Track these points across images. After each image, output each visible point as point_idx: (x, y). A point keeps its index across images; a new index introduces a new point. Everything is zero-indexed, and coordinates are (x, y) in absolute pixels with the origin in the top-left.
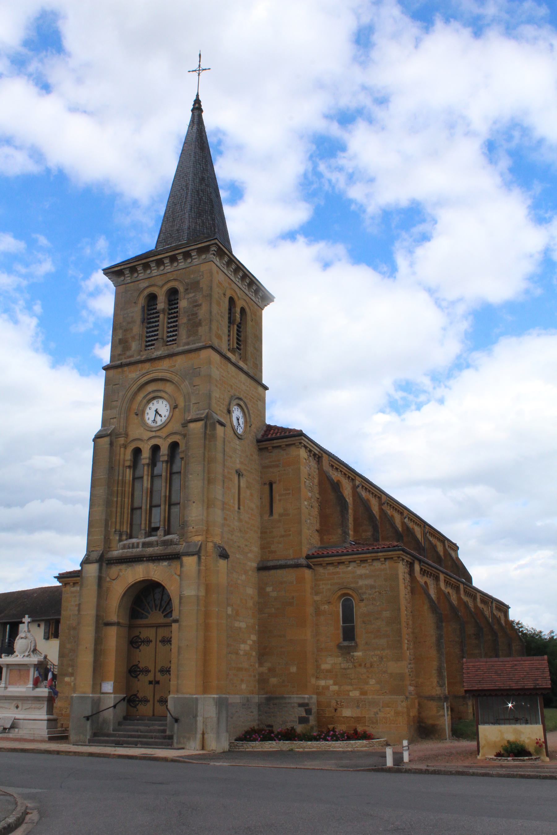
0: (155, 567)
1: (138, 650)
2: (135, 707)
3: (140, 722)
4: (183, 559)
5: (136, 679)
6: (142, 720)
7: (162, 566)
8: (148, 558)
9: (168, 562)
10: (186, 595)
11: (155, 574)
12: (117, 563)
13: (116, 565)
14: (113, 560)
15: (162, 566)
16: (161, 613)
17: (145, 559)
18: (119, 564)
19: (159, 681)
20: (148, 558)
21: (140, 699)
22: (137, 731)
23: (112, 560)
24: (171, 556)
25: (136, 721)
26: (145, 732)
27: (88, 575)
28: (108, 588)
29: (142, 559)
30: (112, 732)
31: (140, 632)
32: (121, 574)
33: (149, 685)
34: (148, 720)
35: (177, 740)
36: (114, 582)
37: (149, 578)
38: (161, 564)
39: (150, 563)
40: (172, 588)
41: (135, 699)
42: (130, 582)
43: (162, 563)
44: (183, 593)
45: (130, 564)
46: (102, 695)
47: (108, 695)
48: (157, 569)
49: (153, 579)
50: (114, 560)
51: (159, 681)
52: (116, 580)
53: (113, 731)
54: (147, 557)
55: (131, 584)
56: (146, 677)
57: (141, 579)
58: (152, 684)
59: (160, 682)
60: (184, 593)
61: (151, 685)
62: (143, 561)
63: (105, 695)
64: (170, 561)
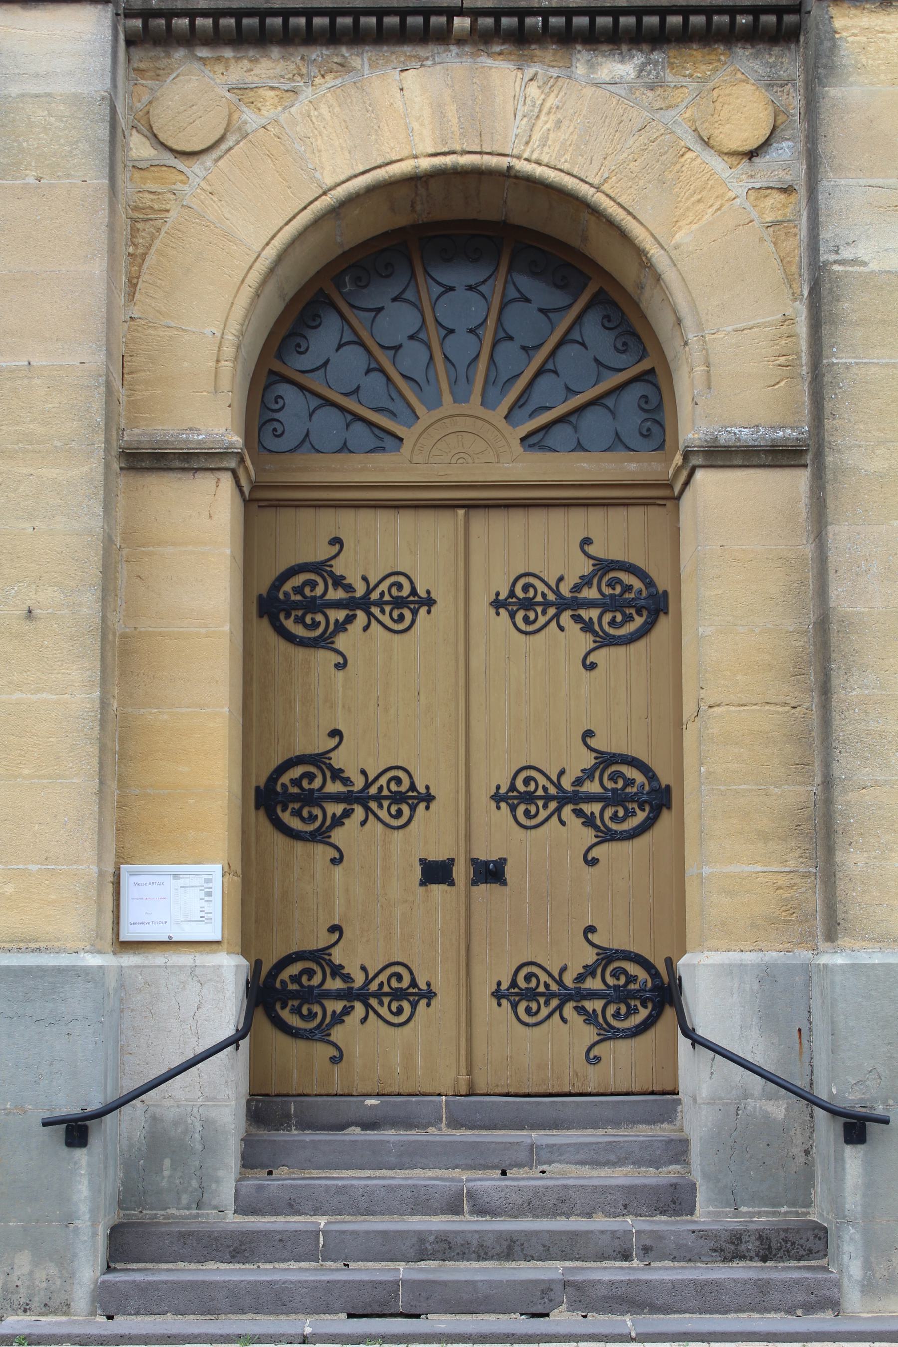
0: (533, 90)
1: (324, 658)
2: (321, 1034)
3: (388, 1135)
4: (838, 24)
5: (322, 852)
6: (406, 1123)
7: (597, 85)
8: (487, 22)
9: (639, 59)
10: (873, 266)
11: (536, 136)
12: (216, 39)
13: (203, 52)
14: (192, 14)
15: (597, 85)
16: (502, 424)
17: (462, 23)
18: (228, 53)
19: (503, 861)
20: (487, 22)
21: (359, 980)
22: (454, 1208)
23: (180, 14)
24: (675, 20)
25: (355, 1133)
26: (517, 1212)
27: (15, 90)
28: (136, 208)
29: (437, 21)
30: (234, 1220)
31: (337, 541)
32: (250, 118)
33: (421, 890)
34: (455, 1123)
35: (867, 1265)
36: (196, 169)
37: (493, 161)
38: (580, 69)
39: (485, 60)
40: (679, 238)
41: (316, 980)
42: (329, 181)
43: (591, 67)
44: (847, 254)
45: (316, 53)
46: (129, 960)
47: (184, 959)
48: (551, 101)
49: (522, 166)
50: (204, 14)
51: (503, 861)
52: (208, 160)
53: (244, 1207)
54: (475, 13)
55: (341, 192)
56: (398, 835)
57: (425, 164)
58: (452, 883)
59: (509, 872)
60: (861, 252)
61: (437, 889)
62: (444, 37)
63: (157, 959)
64: (656, 56)
